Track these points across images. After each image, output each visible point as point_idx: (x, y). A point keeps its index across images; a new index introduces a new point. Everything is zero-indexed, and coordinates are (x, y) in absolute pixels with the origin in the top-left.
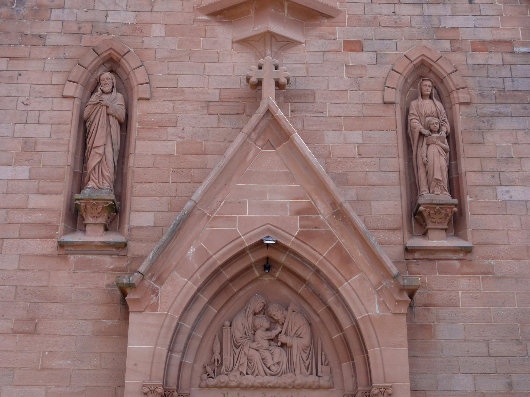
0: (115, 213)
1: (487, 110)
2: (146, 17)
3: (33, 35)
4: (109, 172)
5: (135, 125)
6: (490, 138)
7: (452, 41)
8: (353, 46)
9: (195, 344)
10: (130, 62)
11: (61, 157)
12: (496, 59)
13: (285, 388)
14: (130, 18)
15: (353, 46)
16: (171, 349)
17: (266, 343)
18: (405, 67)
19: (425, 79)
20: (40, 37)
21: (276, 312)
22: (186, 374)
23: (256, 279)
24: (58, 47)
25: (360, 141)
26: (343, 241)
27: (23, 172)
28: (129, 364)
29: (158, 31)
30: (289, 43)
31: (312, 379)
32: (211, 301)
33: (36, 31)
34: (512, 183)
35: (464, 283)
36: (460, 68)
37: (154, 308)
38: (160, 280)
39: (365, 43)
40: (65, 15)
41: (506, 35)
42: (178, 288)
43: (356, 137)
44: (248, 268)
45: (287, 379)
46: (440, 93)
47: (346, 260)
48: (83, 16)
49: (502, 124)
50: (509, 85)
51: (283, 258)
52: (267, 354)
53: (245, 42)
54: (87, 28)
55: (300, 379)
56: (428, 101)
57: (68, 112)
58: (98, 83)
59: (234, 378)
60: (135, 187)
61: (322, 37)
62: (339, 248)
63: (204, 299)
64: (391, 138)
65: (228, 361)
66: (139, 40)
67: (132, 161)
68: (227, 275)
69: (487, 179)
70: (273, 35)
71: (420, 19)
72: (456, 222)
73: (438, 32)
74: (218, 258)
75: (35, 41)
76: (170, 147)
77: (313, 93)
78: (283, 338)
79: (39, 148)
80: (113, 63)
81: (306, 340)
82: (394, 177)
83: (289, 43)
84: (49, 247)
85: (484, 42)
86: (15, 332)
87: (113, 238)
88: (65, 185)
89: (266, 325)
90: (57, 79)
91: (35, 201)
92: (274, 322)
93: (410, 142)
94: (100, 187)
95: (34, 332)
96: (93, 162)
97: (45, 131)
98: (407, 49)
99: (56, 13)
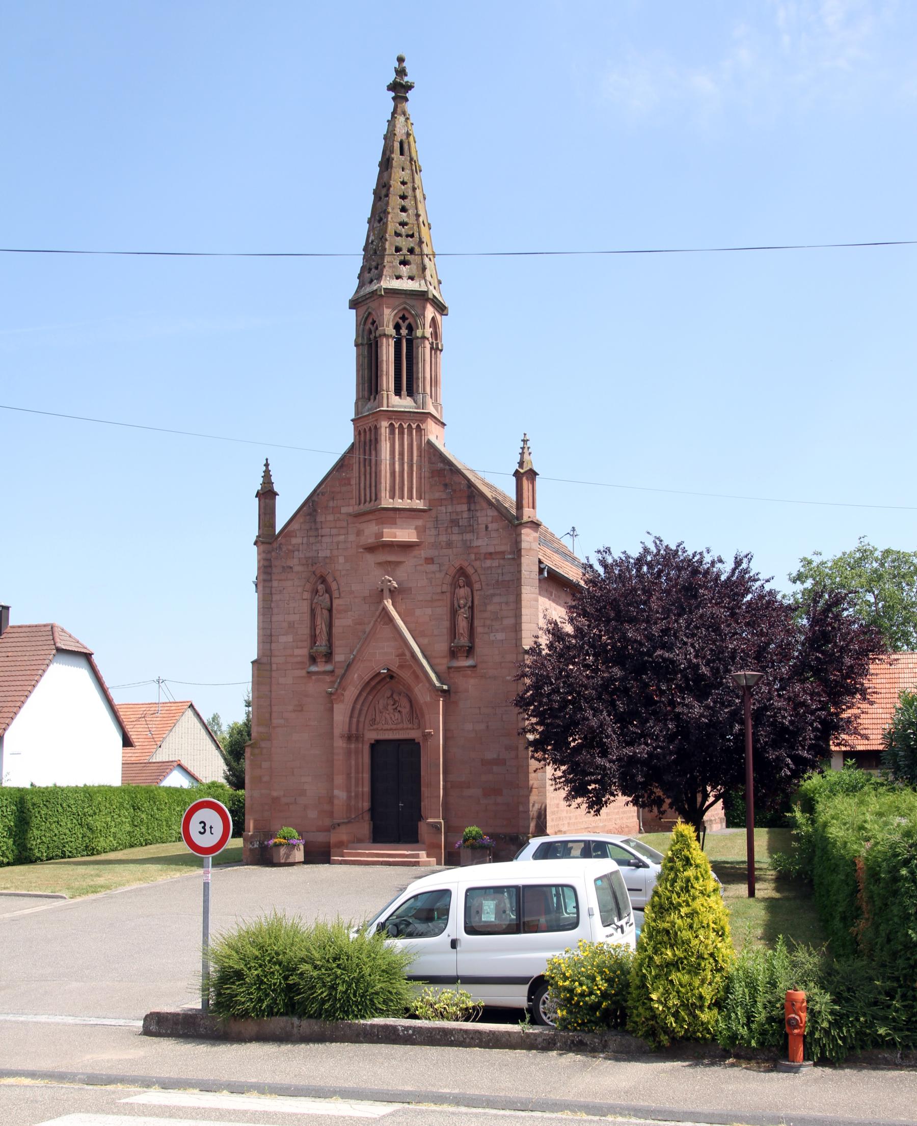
0: (329, 656)
1: (491, 591)
2: (335, 552)
4: (324, 636)
5: (334, 611)
6: (489, 608)
7: (476, 554)
8: (430, 561)
9: (364, 712)
10: (330, 579)
11: (305, 631)
12: (495, 563)
14: (327, 553)
15: (430, 561)
16: (351, 717)
18: (452, 571)
19: (462, 577)
20: (291, 568)
21: (396, 697)
22: (361, 725)
27: (290, 638)
28: (335, 725)
29: (341, 560)
30: (398, 563)
31: (410, 726)
32: (368, 694)
34: (497, 631)
35: (472, 681)
37: (342, 701)
38: (344, 689)
41: (502, 548)
42: (351, 693)
43: (429, 611)
46: (469, 584)
47: (417, 677)
48: (308, 555)
49: (496, 599)
54: (310, 561)
55: (405, 726)
56: (462, 589)
57: (305, 607)
58: (317, 591)
59: (380, 726)
60: (337, 643)
61: (415, 557)
62: (414, 672)
63: (364, 694)
64: (443, 611)
65: (378, 719)
67: (335, 630)
68: (373, 683)
70: (389, 562)
72: (470, 651)
74: (366, 678)
77: (410, 589)
78: (399, 709)
79: (296, 626)
80: (323, 580)
82: (445, 631)
83: (398, 563)
84: (303, 673)
85: (491, 554)
86: (295, 711)
87: (329, 667)
88: (307, 644)
90: (300, 590)
93: (454, 613)
94: (322, 643)
95: (301, 711)
96: (318, 632)
97: (296, 617)
99: (296, 553)
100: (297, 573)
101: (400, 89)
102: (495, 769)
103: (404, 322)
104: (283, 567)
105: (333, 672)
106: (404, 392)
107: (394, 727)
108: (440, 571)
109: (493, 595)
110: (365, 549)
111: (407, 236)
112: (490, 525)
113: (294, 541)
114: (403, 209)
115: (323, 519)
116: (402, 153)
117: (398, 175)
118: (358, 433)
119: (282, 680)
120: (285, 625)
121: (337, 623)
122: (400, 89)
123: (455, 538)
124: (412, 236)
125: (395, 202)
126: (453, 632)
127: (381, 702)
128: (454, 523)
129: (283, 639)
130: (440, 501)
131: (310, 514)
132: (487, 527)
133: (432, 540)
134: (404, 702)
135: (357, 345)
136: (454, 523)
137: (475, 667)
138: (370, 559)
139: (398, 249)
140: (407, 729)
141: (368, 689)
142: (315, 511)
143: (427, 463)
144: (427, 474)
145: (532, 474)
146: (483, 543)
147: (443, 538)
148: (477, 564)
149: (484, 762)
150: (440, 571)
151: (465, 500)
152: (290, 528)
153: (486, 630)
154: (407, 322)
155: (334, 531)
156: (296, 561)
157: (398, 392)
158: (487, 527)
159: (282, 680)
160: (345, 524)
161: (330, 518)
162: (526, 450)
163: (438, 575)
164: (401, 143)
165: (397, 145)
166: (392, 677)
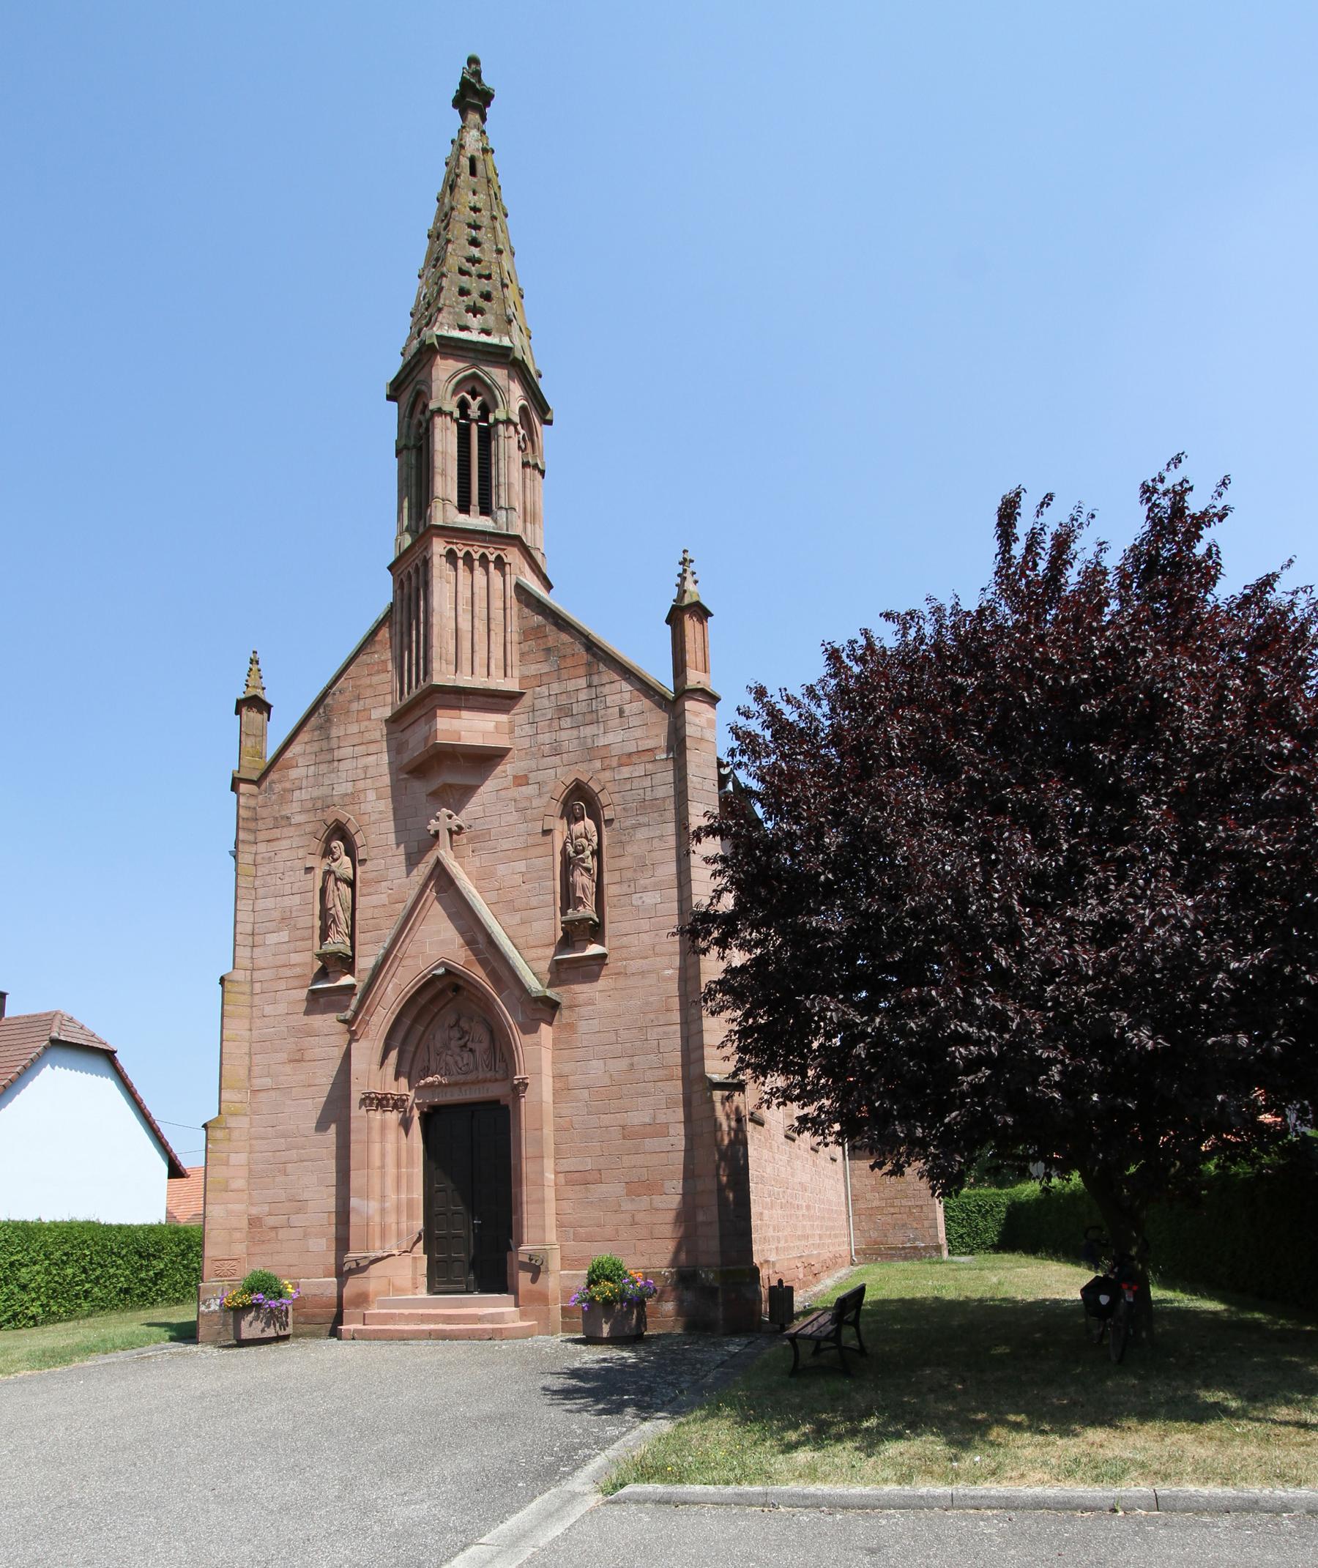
1: (629, 822)
2: (361, 785)
3: (282, 817)
5: (358, 884)
6: (629, 849)
8: (521, 780)
12: (640, 770)
13: (473, 1083)
14: (348, 788)
15: (521, 780)
17: (458, 1050)
18: (560, 792)
19: (580, 801)
23: (451, 1000)
24: (300, 824)
25: (524, 870)
26: (495, 965)
27: (284, 936)
31: (489, 1075)
32: (416, 1020)
33: (283, 813)
34: (645, 890)
36: (608, 785)
39: (531, 775)
40: (303, 795)
43: (521, 866)
44: (442, 992)
45: (470, 1077)
48: (316, 793)
49: (642, 834)
50: (649, 796)
51: (461, 983)
52: (459, 1058)
63: (407, 1022)
66: (357, 807)
68: (422, 1001)
69: (625, 889)
70: (450, 786)
71: (576, 742)
72: (595, 931)
73: (590, 752)
75: (284, 823)
76: (384, 899)
78: (470, 1045)
80: (339, 831)
81: (486, 1044)
85: (630, 754)
86: (290, 1061)
89: (458, 1035)
91: (295, 958)
92: (464, 1033)
95: (302, 1060)
98: (559, 777)
101: (472, 97)
102: (650, 1144)
103: (474, 399)
106: (475, 508)
107: (461, 1078)
108: (540, 795)
109: (635, 827)
111: (480, 276)
112: (627, 708)
113: (294, 773)
114: (474, 242)
115: (342, 733)
116: (473, 172)
117: (466, 198)
118: (399, 585)
119: (268, 1010)
120: (276, 915)
122: (472, 97)
124: (489, 277)
125: (460, 232)
126: (568, 898)
127: (438, 1036)
128: (564, 711)
129: (272, 939)
130: (540, 680)
131: (320, 728)
132: (621, 712)
133: (526, 743)
134: (480, 1032)
135: (398, 453)
136: (564, 711)
139: (463, 292)
140: (485, 1081)
141: (414, 1011)
142: (329, 720)
143: (515, 618)
144: (516, 638)
145: (702, 613)
146: (614, 738)
147: (546, 738)
148: (607, 775)
149: (627, 1133)
150: (540, 795)
151: (582, 671)
152: (288, 754)
153: (624, 888)
154: (479, 399)
156: (296, 807)
157: (464, 507)
158: (621, 712)
159: (268, 1010)
161: (354, 728)
162: (688, 575)
163: (536, 803)
164: (472, 161)
165: (465, 162)
166: (457, 989)
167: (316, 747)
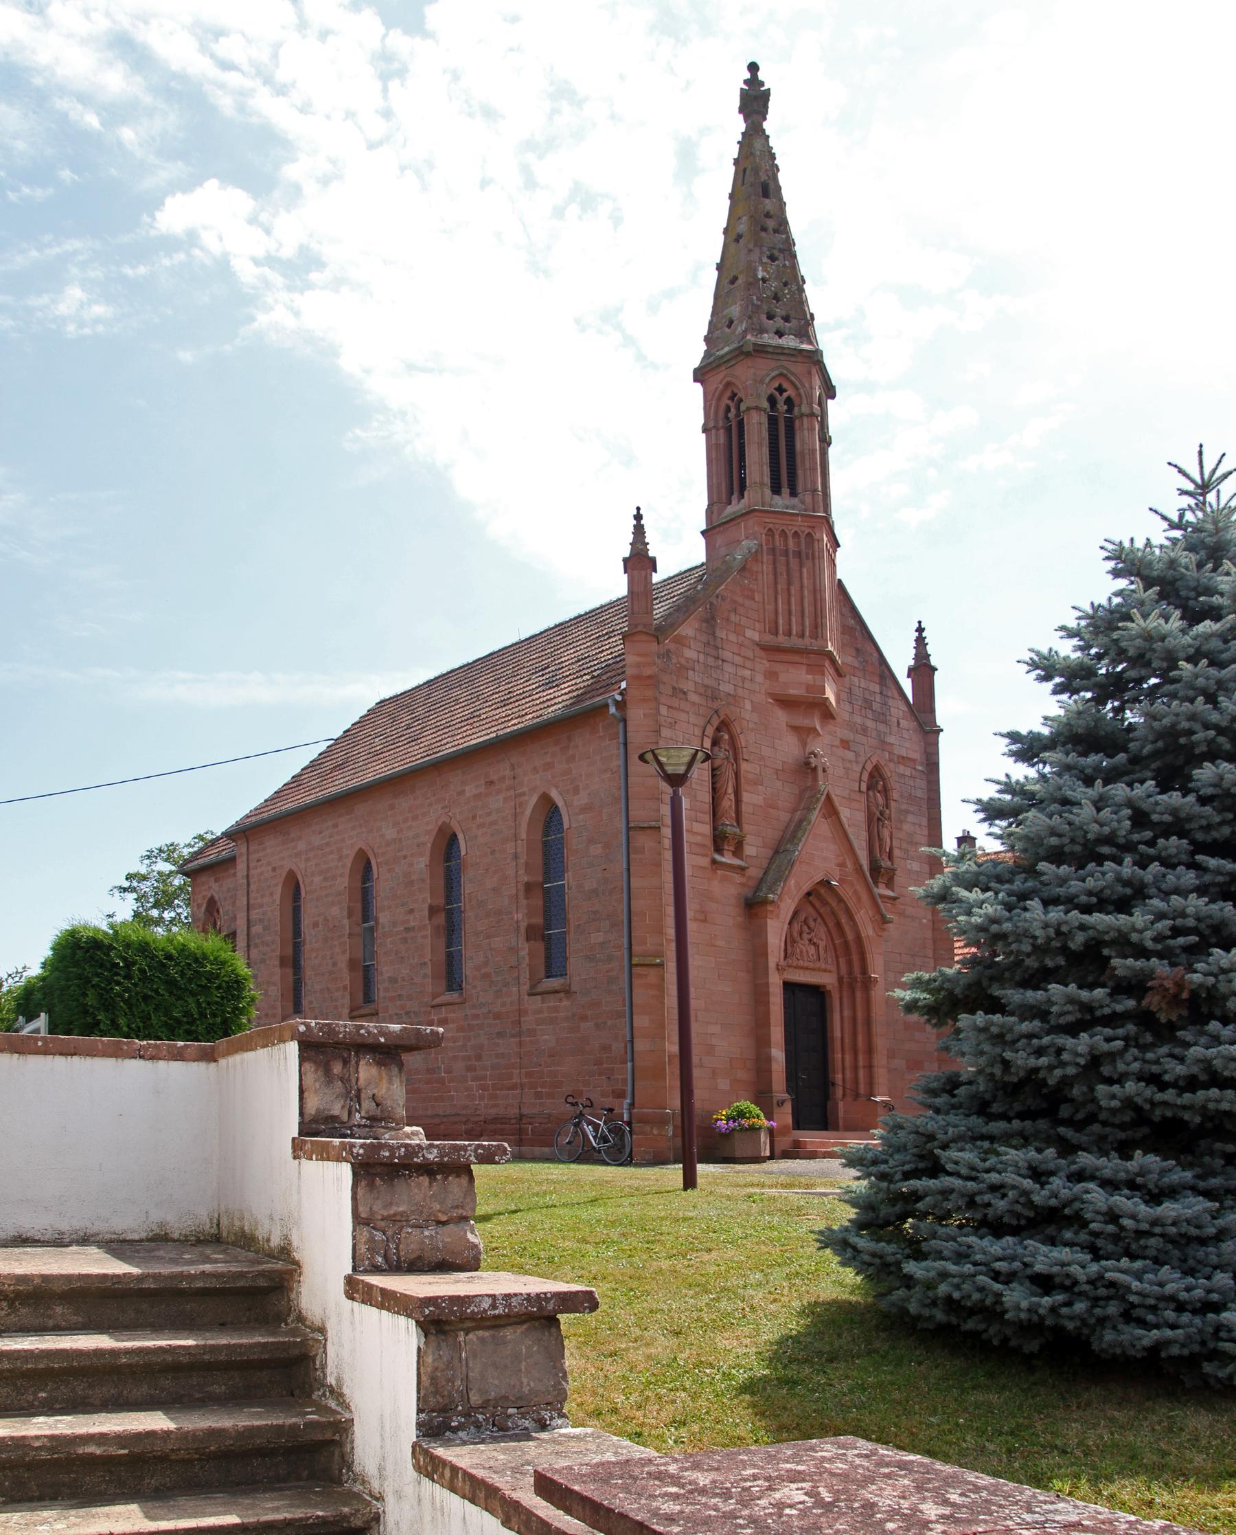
1: (904, 807)
8: (845, 744)
10: (736, 728)
20: (685, 693)
21: (812, 924)
33: (681, 686)
48: (707, 682)
49: (910, 818)
53: (796, 729)
67: (744, 808)
75: (681, 695)
80: (724, 725)
87: (737, 862)
100: (694, 704)
104: (674, 688)
105: (743, 869)
108: (857, 762)
110: (776, 700)
115: (724, 637)
121: (746, 797)
123: (869, 723)
137: (895, 899)
138: (781, 717)
148: (891, 765)
155: (738, 660)
158: (898, 723)
160: (751, 655)
167: (704, 638)
